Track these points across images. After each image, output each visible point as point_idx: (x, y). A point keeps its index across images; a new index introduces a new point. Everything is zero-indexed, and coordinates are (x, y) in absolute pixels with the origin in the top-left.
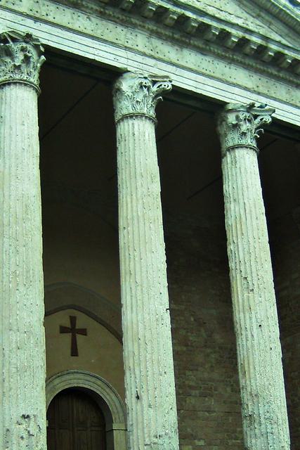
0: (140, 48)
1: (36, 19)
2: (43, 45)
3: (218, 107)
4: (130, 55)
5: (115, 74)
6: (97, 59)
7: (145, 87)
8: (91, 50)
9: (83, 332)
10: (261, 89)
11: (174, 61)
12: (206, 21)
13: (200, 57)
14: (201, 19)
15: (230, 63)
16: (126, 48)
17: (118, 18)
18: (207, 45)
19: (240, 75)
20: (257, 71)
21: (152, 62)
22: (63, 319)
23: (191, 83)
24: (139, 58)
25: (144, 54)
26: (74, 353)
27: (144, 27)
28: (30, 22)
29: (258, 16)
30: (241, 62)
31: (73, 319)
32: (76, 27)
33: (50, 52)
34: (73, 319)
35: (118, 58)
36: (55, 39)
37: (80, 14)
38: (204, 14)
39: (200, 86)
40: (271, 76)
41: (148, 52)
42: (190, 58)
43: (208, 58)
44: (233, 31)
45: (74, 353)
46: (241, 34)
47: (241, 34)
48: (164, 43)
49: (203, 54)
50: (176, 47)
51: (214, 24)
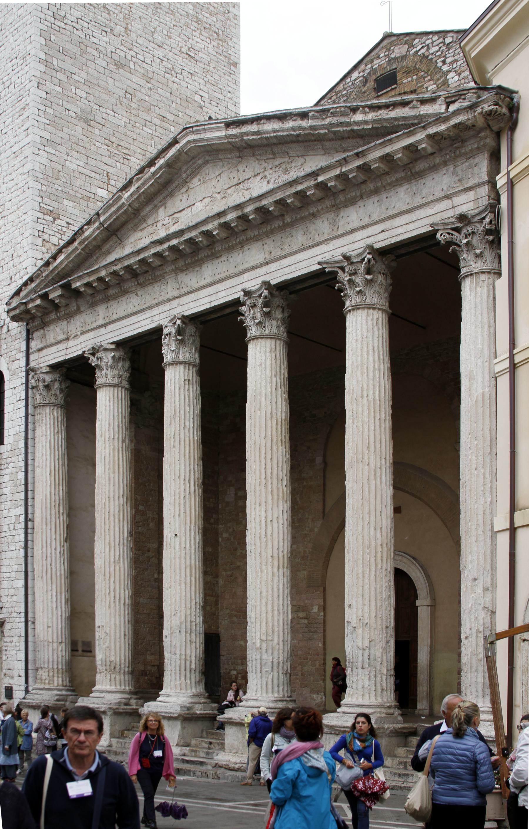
0: (169, 296)
1: (105, 325)
2: (112, 343)
4: (162, 308)
6: (141, 330)
7: (167, 335)
8: (137, 325)
10: (278, 253)
11: (195, 286)
12: (187, 236)
13: (216, 261)
14: (182, 239)
15: (242, 247)
16: (157, 305)
17: (149, 280)
18: (212, 249)
19: (254, 254)
21: (175, 303)
23: (207, 300)
24: (167, 307)
25: (169, 300)
27: (166, 272)
28: (103, 330)
30: (247, 240)
32: (130, 311)
35: (154, 318)
36: (116, 333)
37: (131, 295)
39: (213, 298)
41: (176, 293)
42: (210, 271)
43: (224, 258)
47: (216, 223)
48: (187, 272)
49: (217, 258)
50: (197, 269)
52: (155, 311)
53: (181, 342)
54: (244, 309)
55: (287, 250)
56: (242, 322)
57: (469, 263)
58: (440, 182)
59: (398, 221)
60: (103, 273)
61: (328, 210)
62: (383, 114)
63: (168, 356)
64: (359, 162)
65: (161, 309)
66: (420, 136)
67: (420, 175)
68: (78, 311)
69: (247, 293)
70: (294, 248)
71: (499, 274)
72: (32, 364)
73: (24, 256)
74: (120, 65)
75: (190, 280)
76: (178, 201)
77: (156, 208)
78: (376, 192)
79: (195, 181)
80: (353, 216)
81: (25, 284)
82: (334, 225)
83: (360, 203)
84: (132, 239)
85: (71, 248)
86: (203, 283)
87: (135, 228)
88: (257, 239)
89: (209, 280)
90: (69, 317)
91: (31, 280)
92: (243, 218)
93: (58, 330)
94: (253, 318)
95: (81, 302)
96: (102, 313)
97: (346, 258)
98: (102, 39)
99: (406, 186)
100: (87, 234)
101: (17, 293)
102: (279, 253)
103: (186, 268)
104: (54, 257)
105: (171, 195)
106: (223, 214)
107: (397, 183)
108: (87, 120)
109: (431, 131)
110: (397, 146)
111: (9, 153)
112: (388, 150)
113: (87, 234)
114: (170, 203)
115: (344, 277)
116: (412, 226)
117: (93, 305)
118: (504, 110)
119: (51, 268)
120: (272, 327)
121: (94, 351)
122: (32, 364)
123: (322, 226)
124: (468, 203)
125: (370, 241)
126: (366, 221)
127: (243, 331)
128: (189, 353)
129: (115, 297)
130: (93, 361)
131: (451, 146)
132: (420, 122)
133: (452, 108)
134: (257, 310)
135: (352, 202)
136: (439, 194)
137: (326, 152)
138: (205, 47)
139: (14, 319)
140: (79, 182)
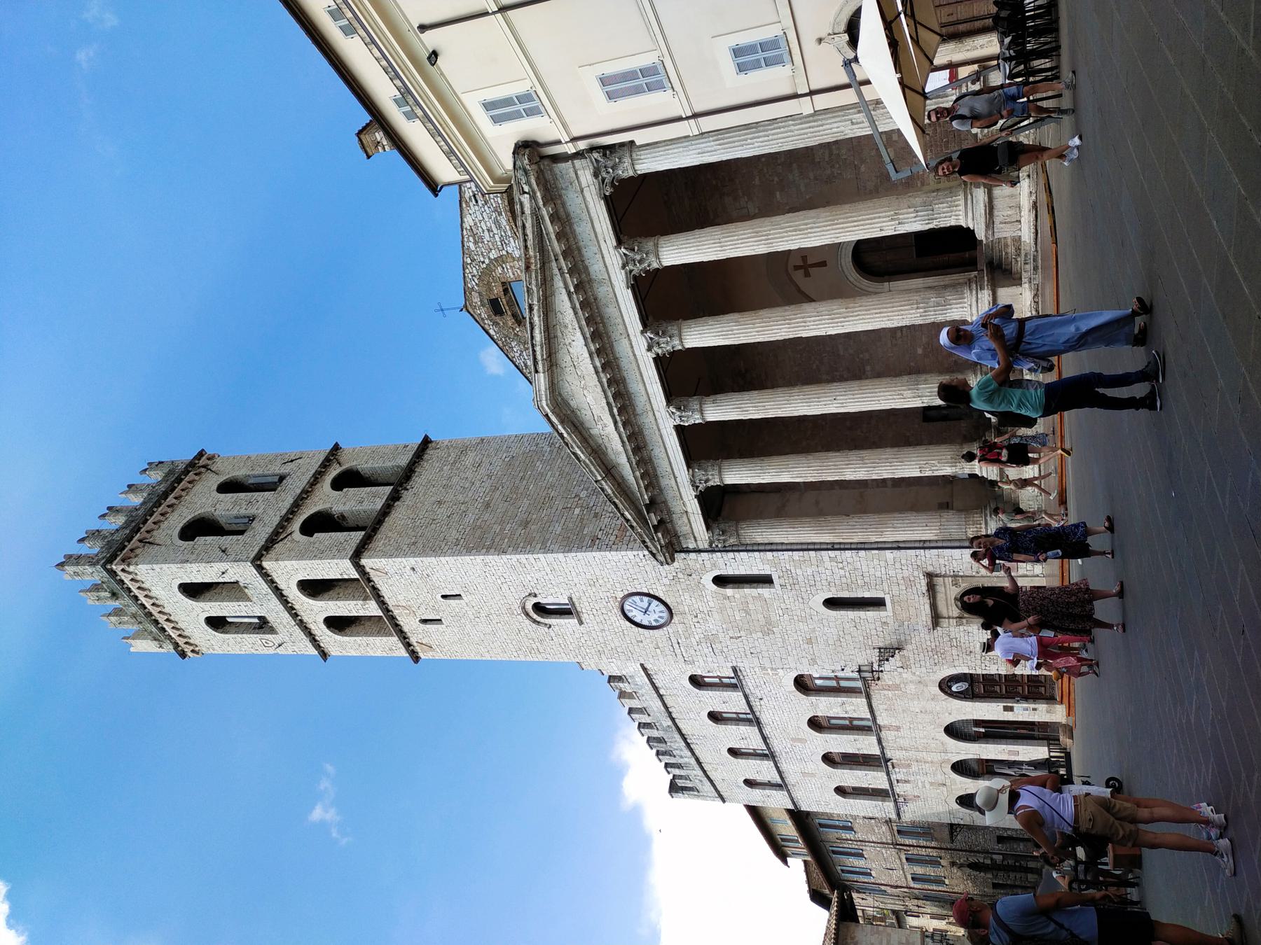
1: (675, 478)
3: (658, 360)
5: (679, 429)
9: (804, 258)
11: (645, 397)
12: (611, 400)
19: (622, 348)
20: (609, 337)
22: (798, 276)
24: (660, 421)
26: (823, 264)
29: (556, 337)
31: (797, 268)
33: (689, 467)
34: (797, 268)
38: (608, 404)
40: (604, 326)
41: (650, 414)
42: (635, 387)
44: (605, 380)
45: (823, 264)
46: (602, 375)
51: (610, 395)
52: (664, 432)
53: (686, 409)
54: (660, 351)
55: (619, 320)
56: (670, 353)
57: (626, 171)
58: (573, 201)
59: (598, 230)
60: (638, 474)
61: (591, 287)
62: (530, 243)
63: (696, 419)
64: (561, 258)
65: (663, 422)
66: (544, 212)
67: (568, 215)
68: (665, 502)
69: (649, 349)
70: (618, 314)
71: (632, 142)
72: (706, 546)
73: (626, 558)
74: (488, 505)
75: (640, 402)
76: (586, 415)
77: (591, 436)
78: (579, 249)
79: (572, 403)
80: (596, 268)
81: (647, 547)
82: (601, 282)
83: (587, 262)
84: (613, 457)
85: (621, 506)
86: (643, 392)
87: (605, 454)
88: (612, 346)
89: (641, 386)
90: (670, 513)
91: (644, 542)
92: (599, 352)
93: (680, 522)
94: (667, 343)
95: (658, 500)
96: (667, 482)
97: (623, 267)
98: (471, 517)
99: (575, 227)
100: (610, 491)
101: (654, 555)
102: (621, 327)
103: (632, 405)
104: (628, 521)
105: (582, 424)
106: (595, 368)
107: (573, 232)
108: (526, 524)
109: (541, 203)
110: (550, 228)
111: (551, 576)
112: (553, 236)
113: (610, 491)
114: (587, 425)
115: (637, 268)
116: (602, 218)
117: (661, 490)
118: (527, 151)
119: (635, 524)
120: (673, 329)
121: (696, 487)
122: (706, 546)
123: (602, 292)
124: (586, 177)
125: (611, 250)
126: (599, 256)
127: (674, 353)
128: (694, 403)
129: (655, 469)
130: (702, 487)
131: (551, 193)
132: (536, 214)
133: (526, 189)
134: (662, 340)
135: (586, 268)
136: (581, 198)
137: (553, 294)
138: (470, 459)
139: (673, 560)
140: (571, 525)
